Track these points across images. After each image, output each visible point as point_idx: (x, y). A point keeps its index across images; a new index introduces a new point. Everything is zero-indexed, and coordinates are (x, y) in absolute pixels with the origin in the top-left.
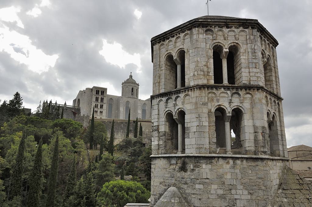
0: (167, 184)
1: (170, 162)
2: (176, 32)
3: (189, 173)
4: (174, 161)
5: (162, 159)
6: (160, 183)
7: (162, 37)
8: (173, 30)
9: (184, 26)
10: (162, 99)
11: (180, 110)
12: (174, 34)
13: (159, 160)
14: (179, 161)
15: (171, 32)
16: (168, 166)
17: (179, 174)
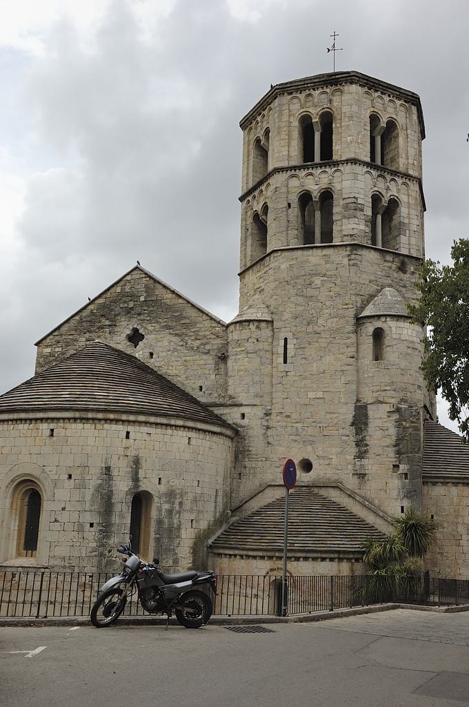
0: (380, 284)
1: (384, 257)
2: (391, 92)
3: (408, 275)
4: (389, 258)
5: (372, 251)
6: (370, 282)
7: (372, 84)
8: (389, 87)
9: (405, 94)
10: (372, 171)
11: (392, 197)
12: (388, 91)
13: (368, 251)
14: (396, 260)
15: (386, 87)
16: (381, 262)
17: (396, 275)
